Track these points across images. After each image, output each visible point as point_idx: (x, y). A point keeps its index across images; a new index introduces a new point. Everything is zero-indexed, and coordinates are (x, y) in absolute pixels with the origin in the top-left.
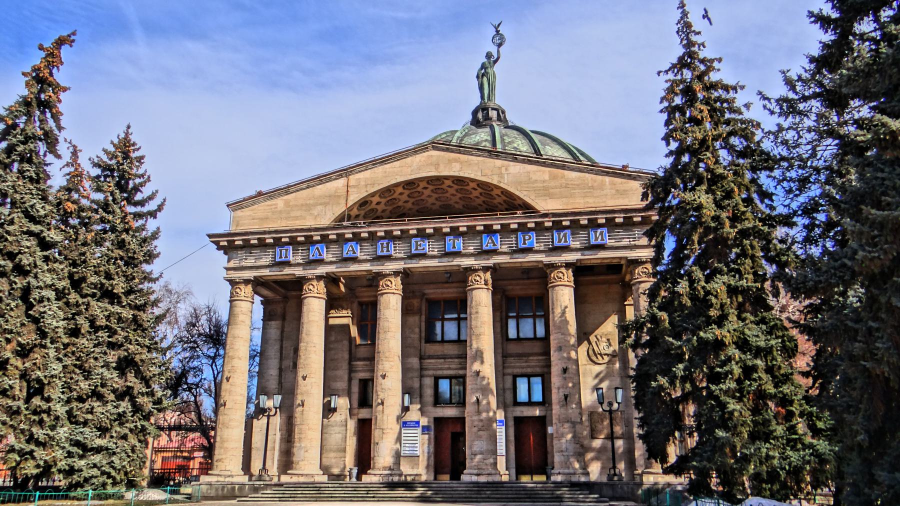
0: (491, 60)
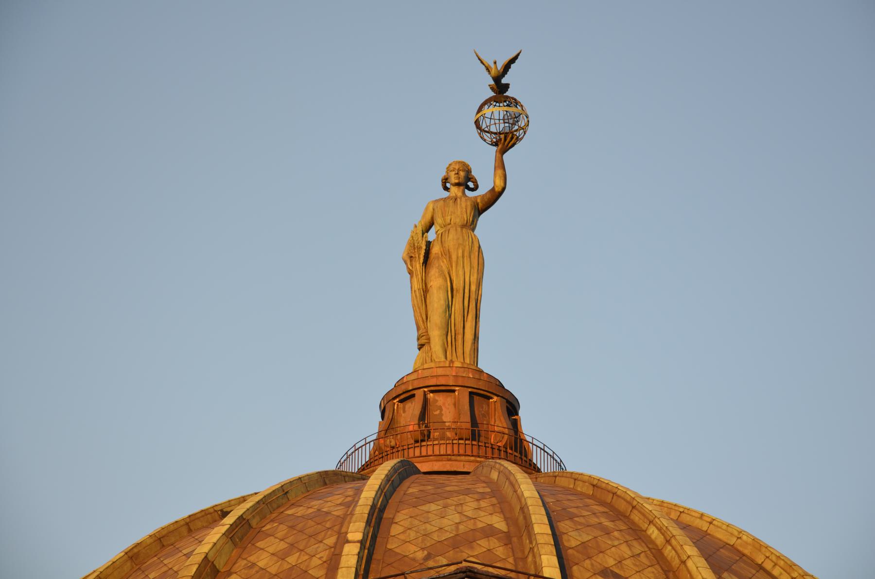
0: (471, 198)
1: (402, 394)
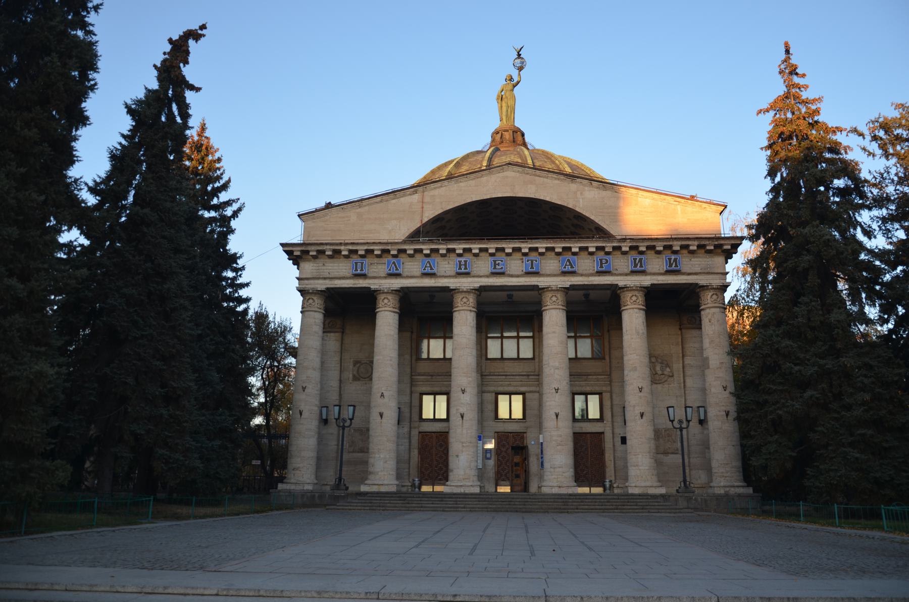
0: (512, 83)
1: (496, 132)
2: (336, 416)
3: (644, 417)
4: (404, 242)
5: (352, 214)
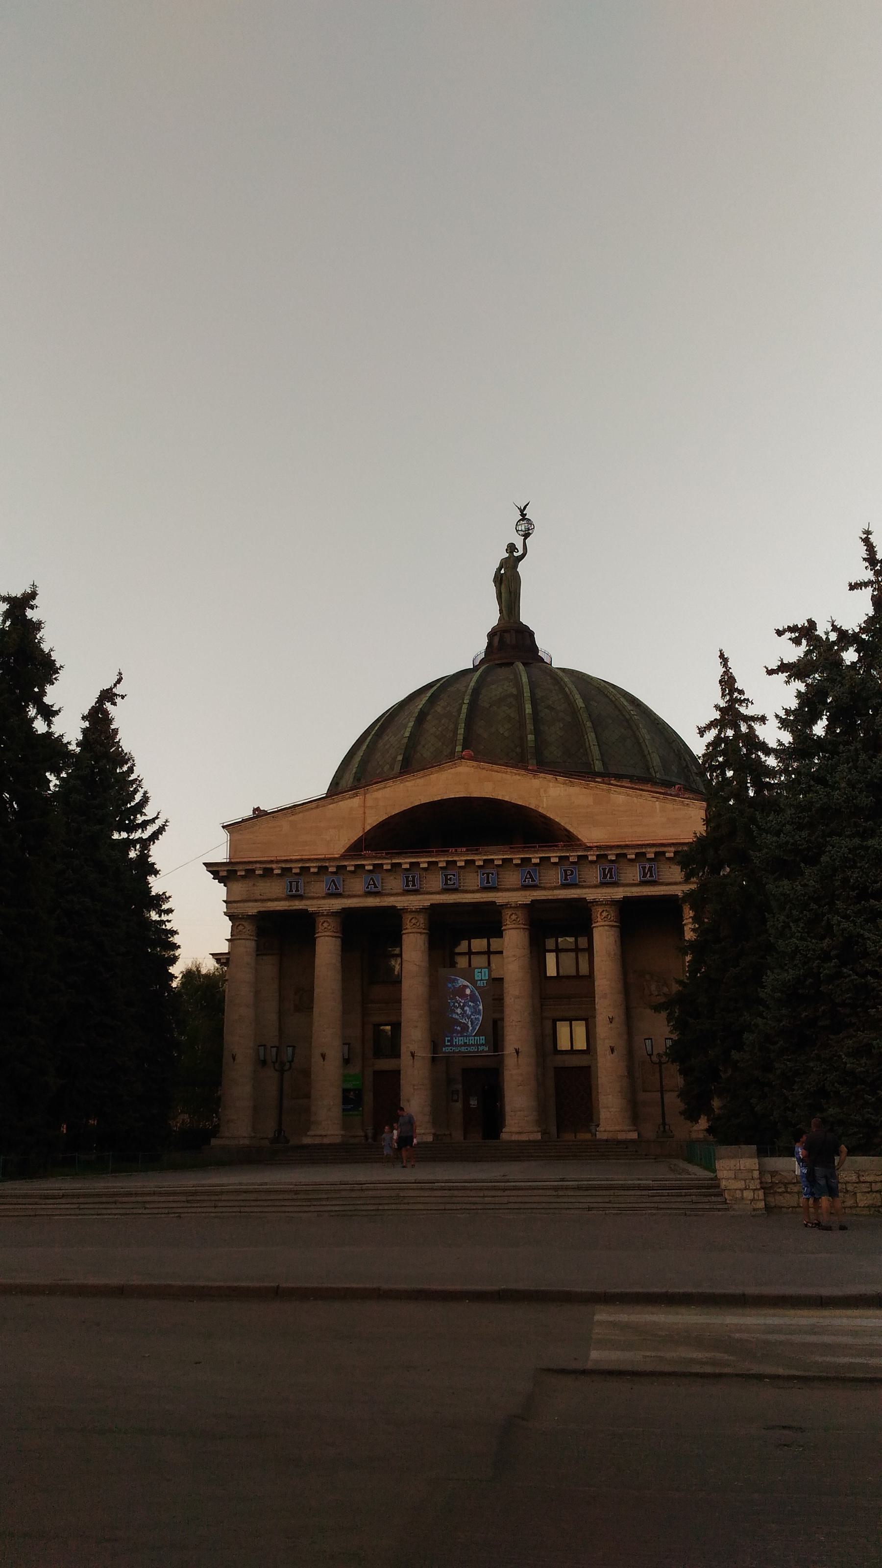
2: (274, 1059)
3: (615, 1052)
4: (343, 857)
5: (285, 824)
